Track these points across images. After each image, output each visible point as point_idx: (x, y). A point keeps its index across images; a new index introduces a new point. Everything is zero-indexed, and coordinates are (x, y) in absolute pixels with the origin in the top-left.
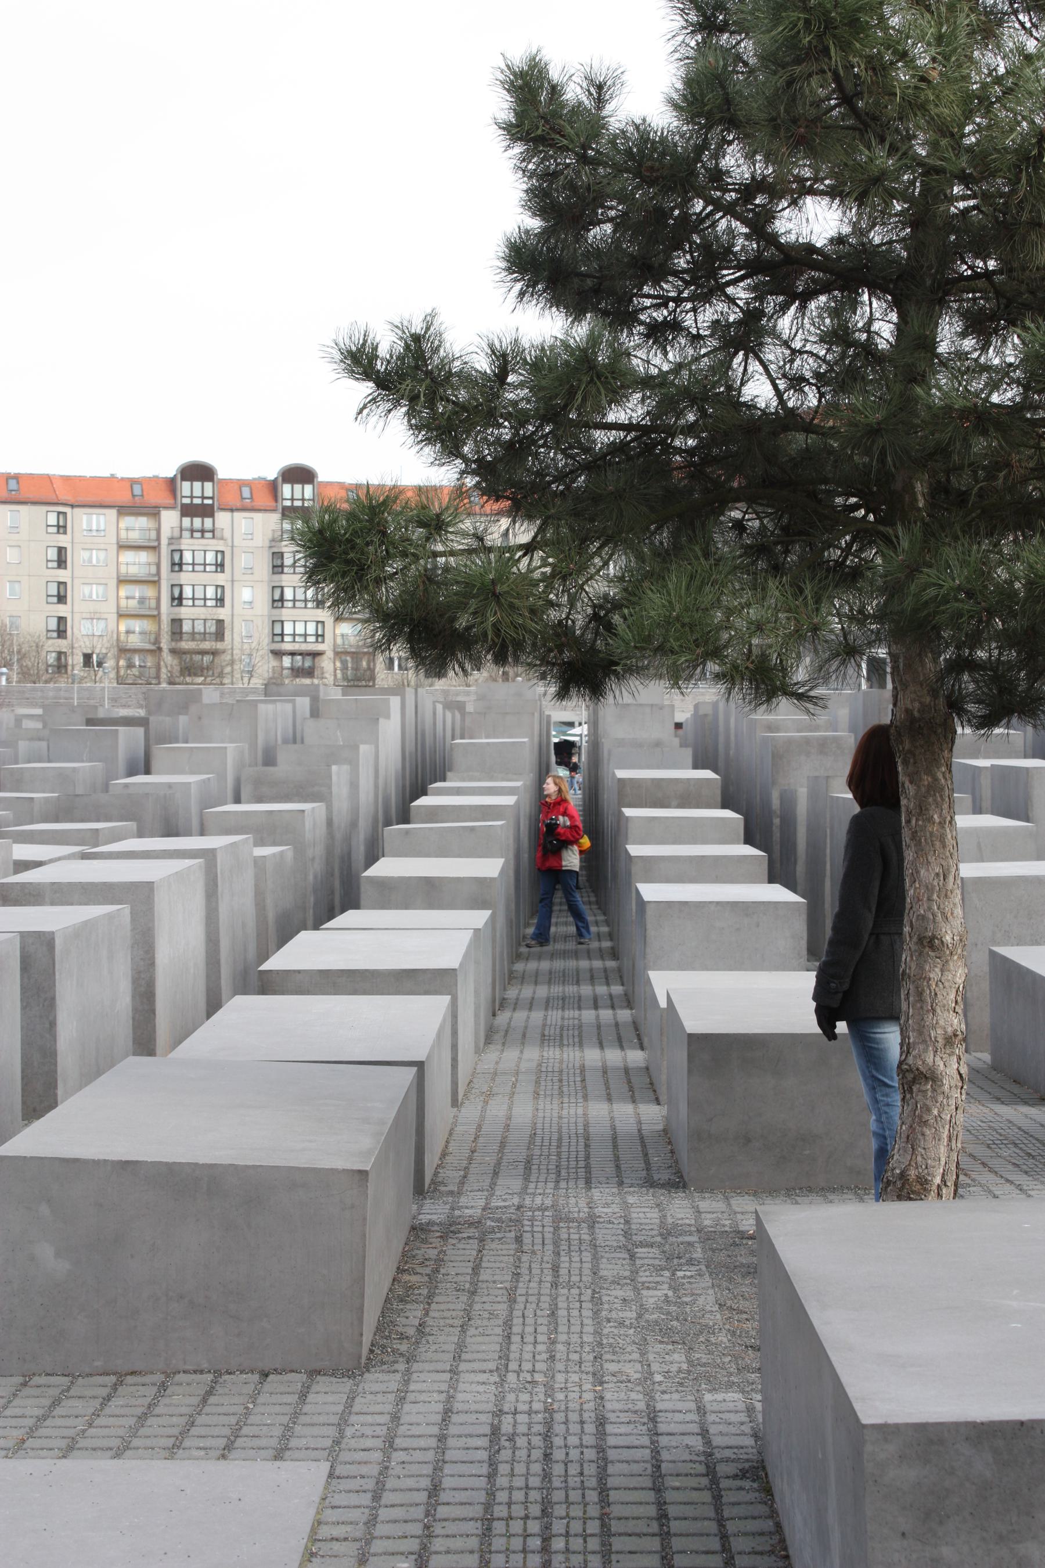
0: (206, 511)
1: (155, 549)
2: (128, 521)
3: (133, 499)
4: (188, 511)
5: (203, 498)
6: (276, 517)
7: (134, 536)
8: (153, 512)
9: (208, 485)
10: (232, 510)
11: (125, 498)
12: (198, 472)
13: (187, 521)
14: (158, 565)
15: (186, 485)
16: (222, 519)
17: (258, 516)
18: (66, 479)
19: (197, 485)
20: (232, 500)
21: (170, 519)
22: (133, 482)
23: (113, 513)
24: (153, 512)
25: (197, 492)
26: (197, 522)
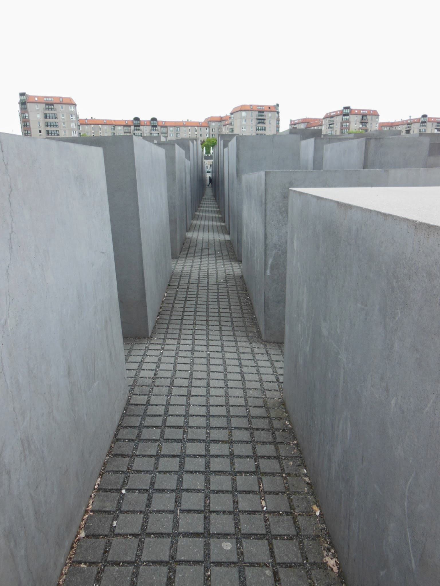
0: (139, 126)
1: (130, 133)
2: (125, 128)
4: (135, 126)
6: (150, 127)
7: (127, 131)
8: (130, 126)
11: (124, 124)
17: (147, 127)
20: (142, 124)
21: (132, 128)
22: (126, 121)
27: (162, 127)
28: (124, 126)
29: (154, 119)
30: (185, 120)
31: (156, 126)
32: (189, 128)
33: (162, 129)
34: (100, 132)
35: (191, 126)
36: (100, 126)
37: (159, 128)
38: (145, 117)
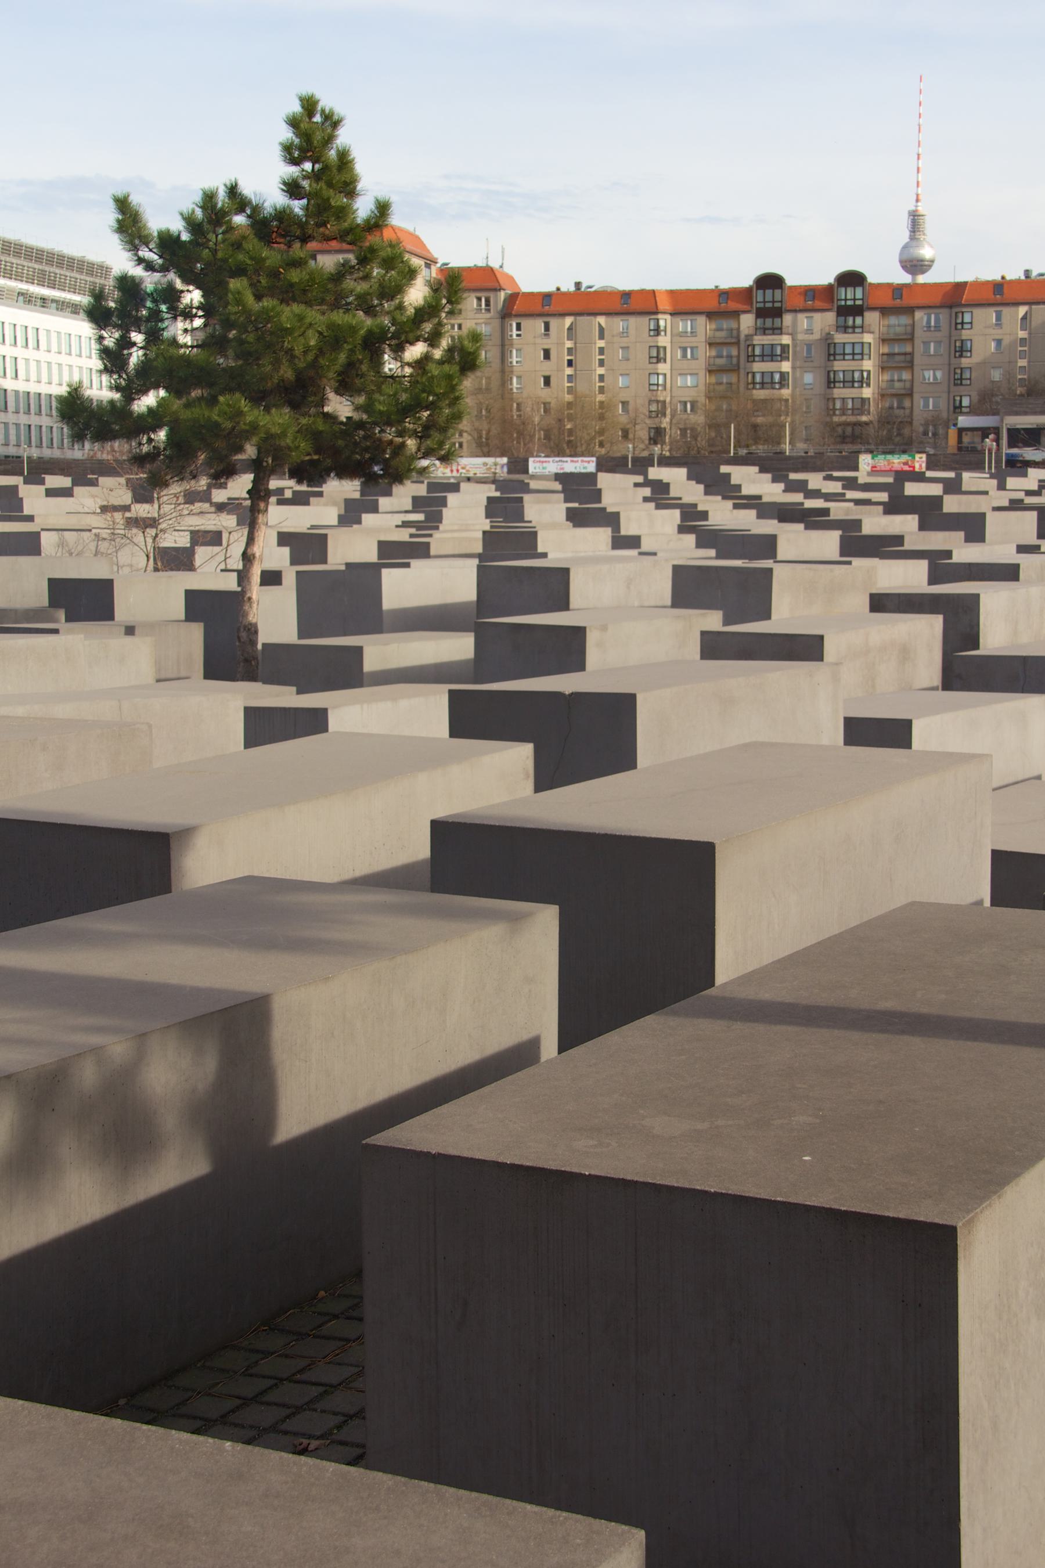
1: (737, 343)
3: (719, 305)
5: (764, 302)
9: (778, 292)
10: (795, 311)
11: (712, 305)
12: (770, 282)
13: (760, 321)
14: (738, 356)
15: (760, 292)
16: (788, 319)
17: (817, 316)
18: (672, 293)
19: (769, 292)
20: (799, 302)
21: (747, 321)
23: (701, 320)
24: (736, 314)
25: (769, 298)
26: (769, 322)
27: (885, 311)
28: (710, 315)
29: (852, 279)
30: (1015, 274)
31: (857, 311)
32: (1022, 310)
33: (893, 320)
34: (601, 344)
35: (1030, 304)
36: (602, 320)
37: (872, 318)
38: (809, 269)
